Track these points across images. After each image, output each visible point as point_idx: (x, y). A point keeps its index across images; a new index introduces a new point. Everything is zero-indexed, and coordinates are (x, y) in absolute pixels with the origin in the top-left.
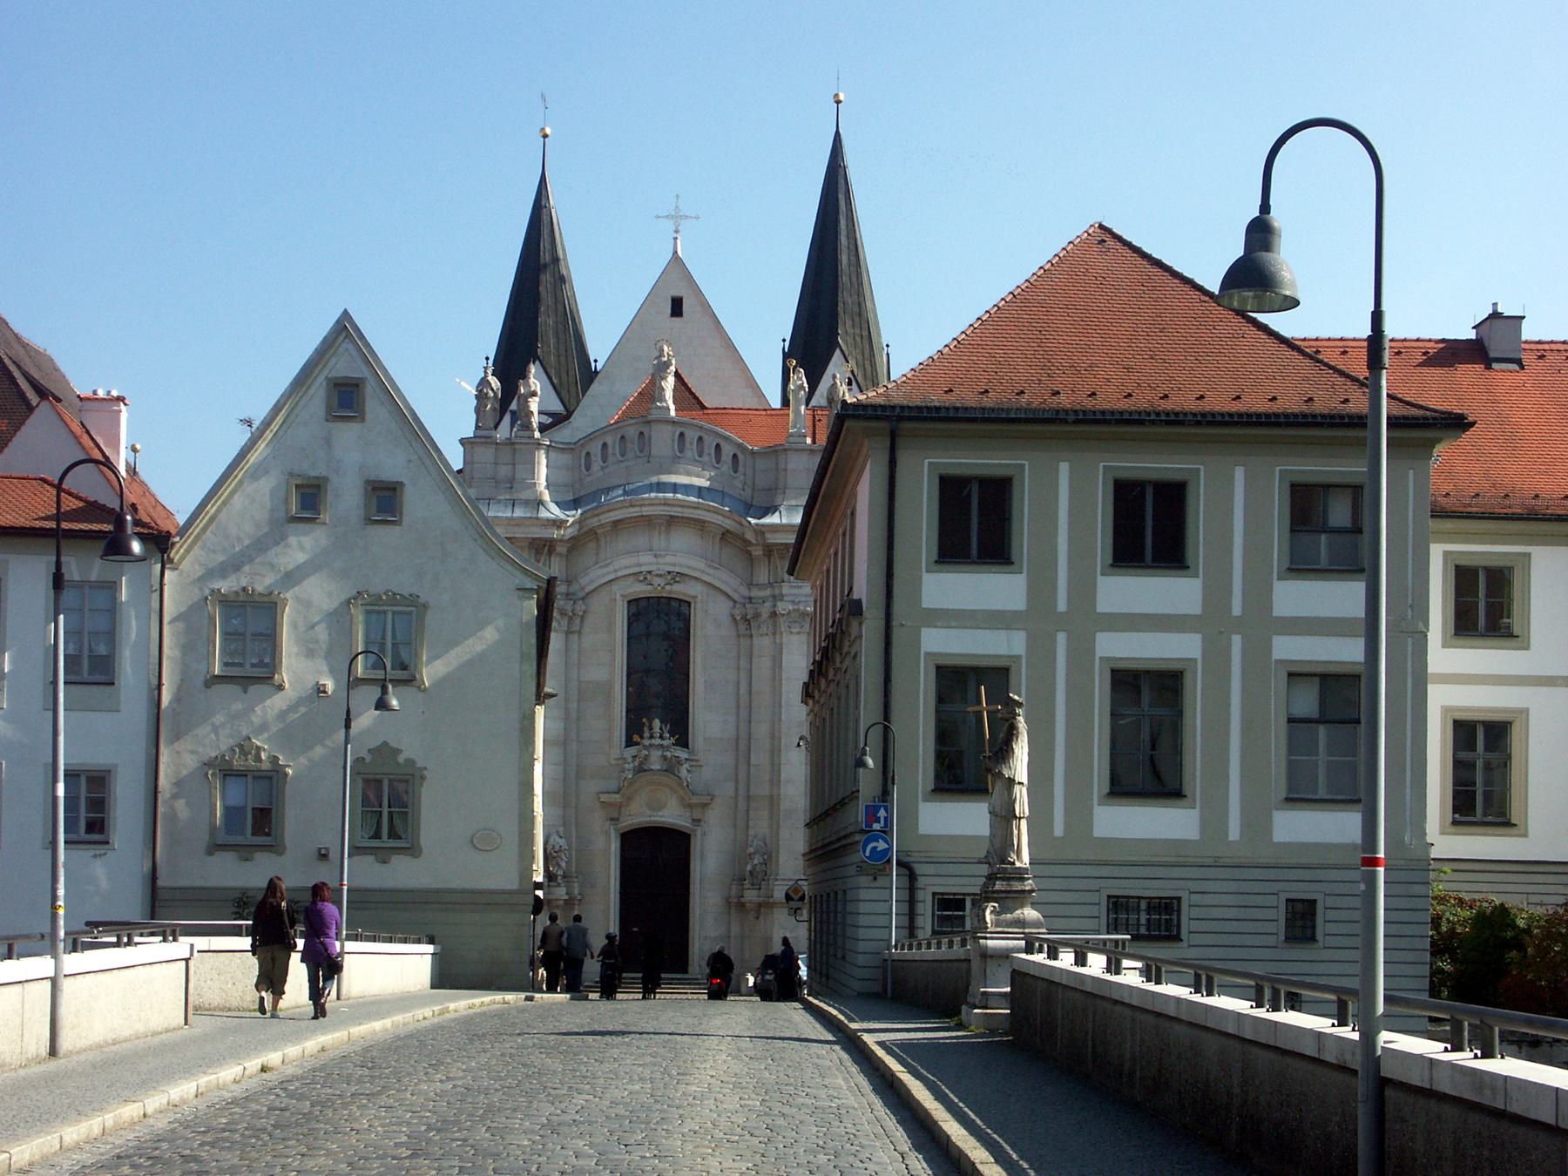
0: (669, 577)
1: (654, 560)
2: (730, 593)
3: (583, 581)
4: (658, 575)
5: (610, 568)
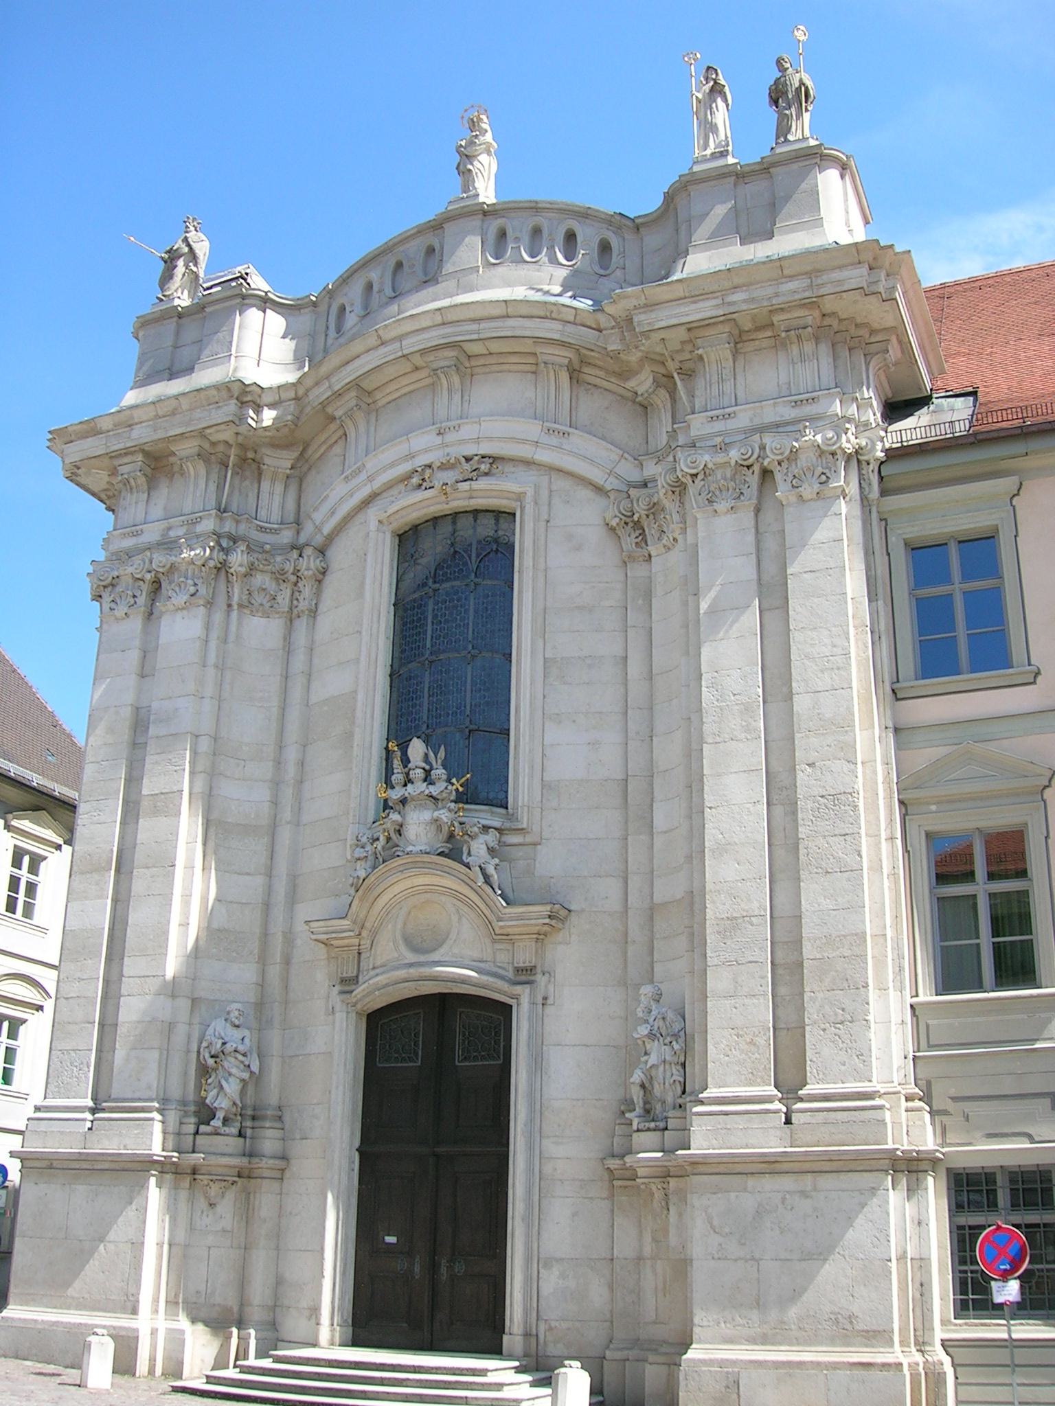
0: (467, 466)
1: (438, 440)
2: (597, 476)
3: (318, 517)
4: (444, 467)
5: (363, 476)
